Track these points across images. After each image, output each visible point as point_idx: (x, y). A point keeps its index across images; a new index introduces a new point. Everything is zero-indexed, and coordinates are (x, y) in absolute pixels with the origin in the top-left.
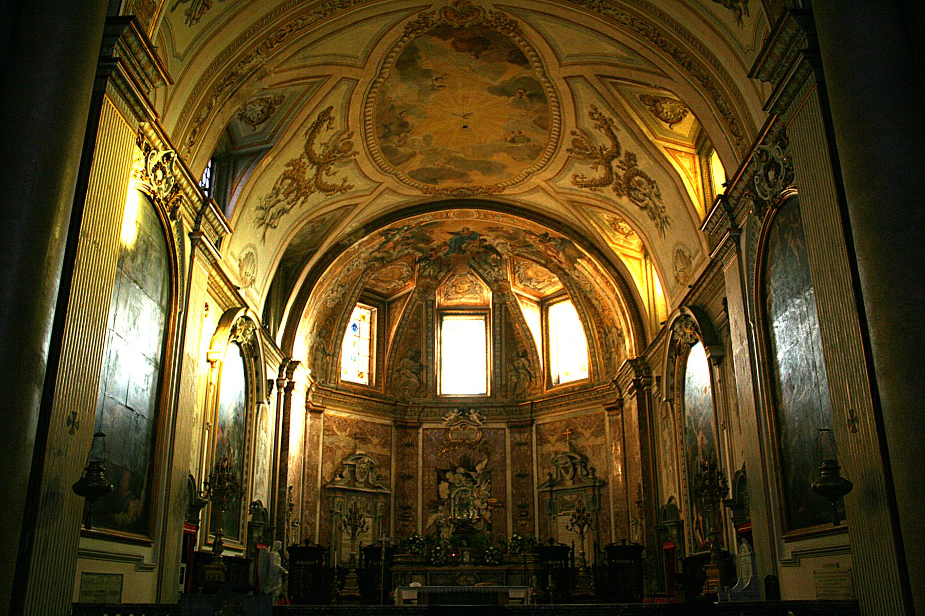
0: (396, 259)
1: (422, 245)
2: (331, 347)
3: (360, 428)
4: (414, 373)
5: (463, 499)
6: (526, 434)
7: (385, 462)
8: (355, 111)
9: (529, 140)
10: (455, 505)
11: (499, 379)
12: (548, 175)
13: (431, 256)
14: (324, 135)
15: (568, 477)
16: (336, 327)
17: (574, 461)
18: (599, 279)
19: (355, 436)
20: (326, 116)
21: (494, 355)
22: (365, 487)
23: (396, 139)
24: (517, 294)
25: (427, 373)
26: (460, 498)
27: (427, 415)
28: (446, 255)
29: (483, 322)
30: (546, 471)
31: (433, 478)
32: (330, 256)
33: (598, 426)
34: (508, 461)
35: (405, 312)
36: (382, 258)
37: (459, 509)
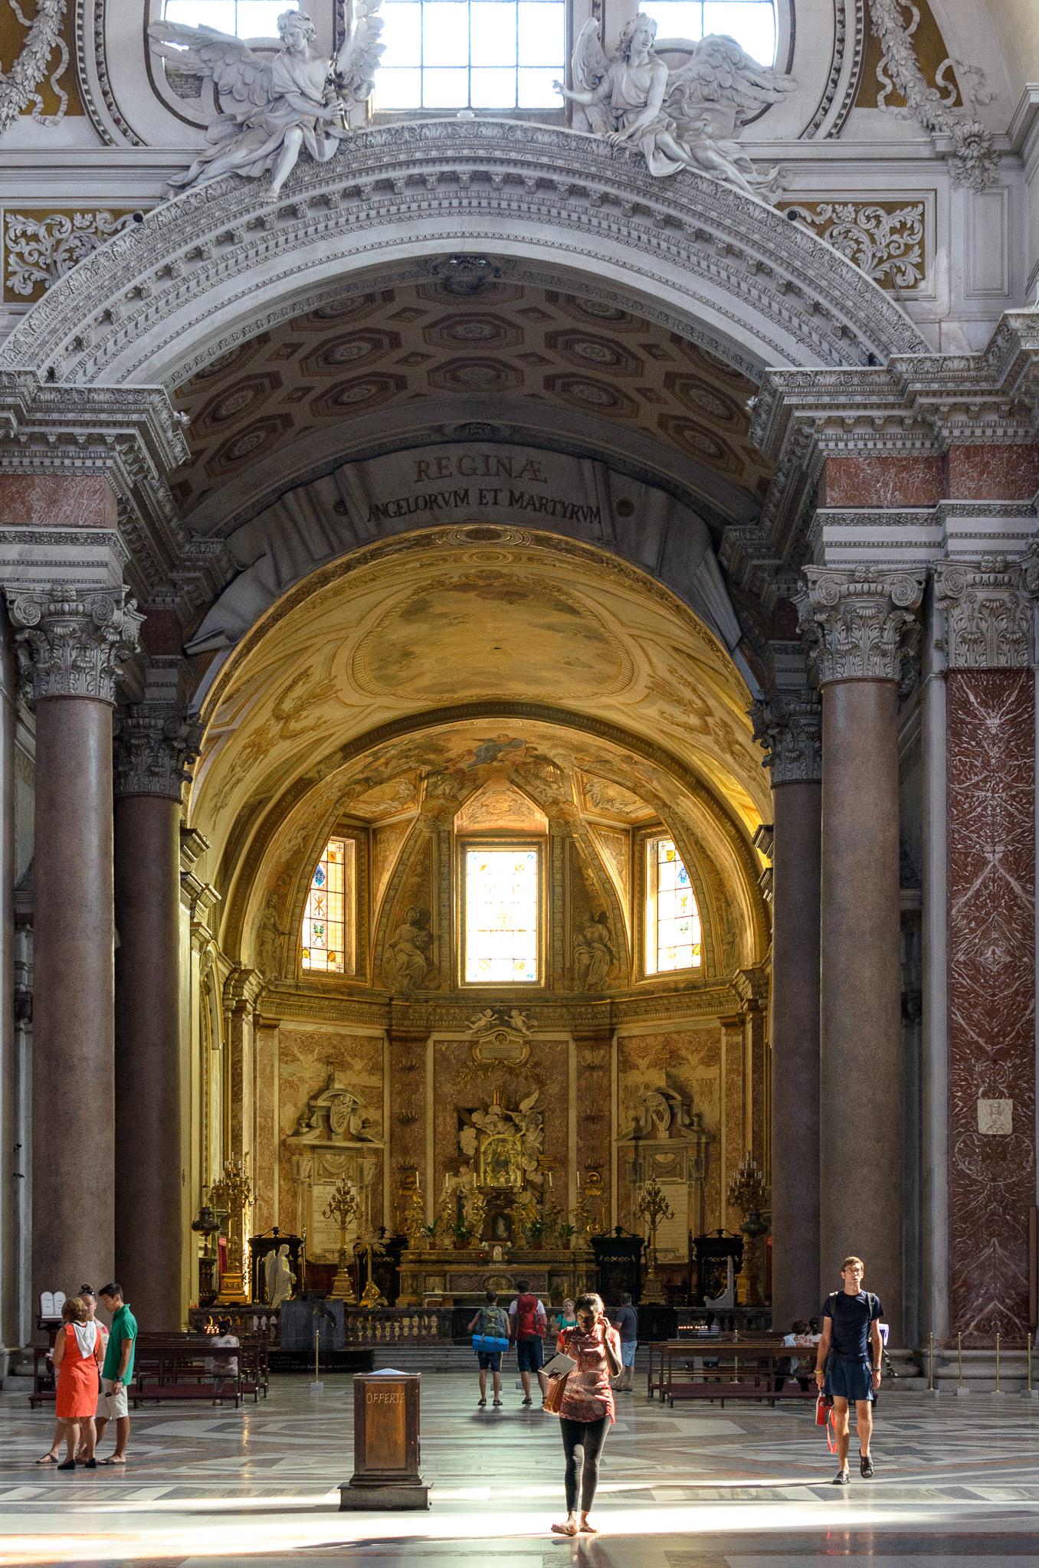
0: (389, 778)
1: (432, 756)
2: (287, 920)
3: (334, 1047)
4: (418, 948)
5: (500, 1155)
6: (602, 1052)
7: (373, 1097)
8: (343, 657)
9: (591, 667)
10: (487, 1164)
11: (559, 958)
12: (621, 699)
13: (447, 768)
14: (299, 690)
15: (662, 1126)
16: (294, 889)
17: (672, 1102)
18: (710, 831)
19: (328, 1061)
20: (305, 674)
21: (553, 920)
22: (345, 1139)
23: (396, 667)
24: (590, 823)
25: (440, 948)
26: (495, 1153)
27: (441, 1019)
28: (470, 766)
29: (534, 855)
30: (632, 1113)
31: (451, 1121)
32: (289, 798)
33: (709, 1049)
34: (573, 1094)
35: (403, 851)
36: (367, 780)
37: (493, 1171)
